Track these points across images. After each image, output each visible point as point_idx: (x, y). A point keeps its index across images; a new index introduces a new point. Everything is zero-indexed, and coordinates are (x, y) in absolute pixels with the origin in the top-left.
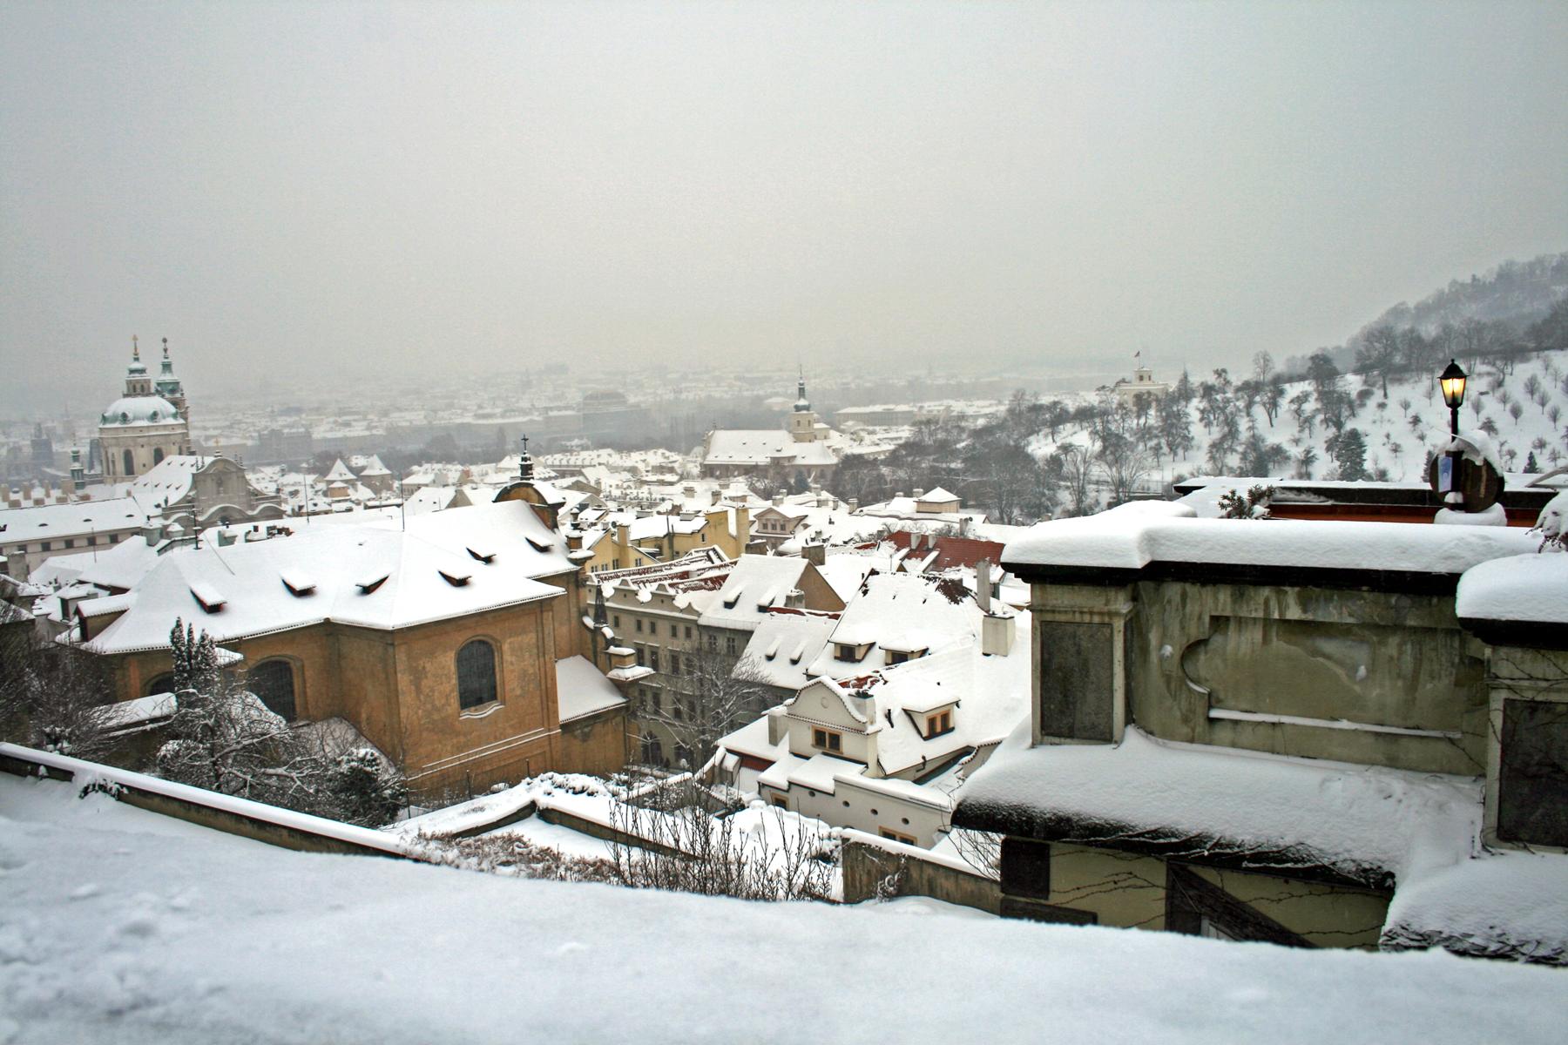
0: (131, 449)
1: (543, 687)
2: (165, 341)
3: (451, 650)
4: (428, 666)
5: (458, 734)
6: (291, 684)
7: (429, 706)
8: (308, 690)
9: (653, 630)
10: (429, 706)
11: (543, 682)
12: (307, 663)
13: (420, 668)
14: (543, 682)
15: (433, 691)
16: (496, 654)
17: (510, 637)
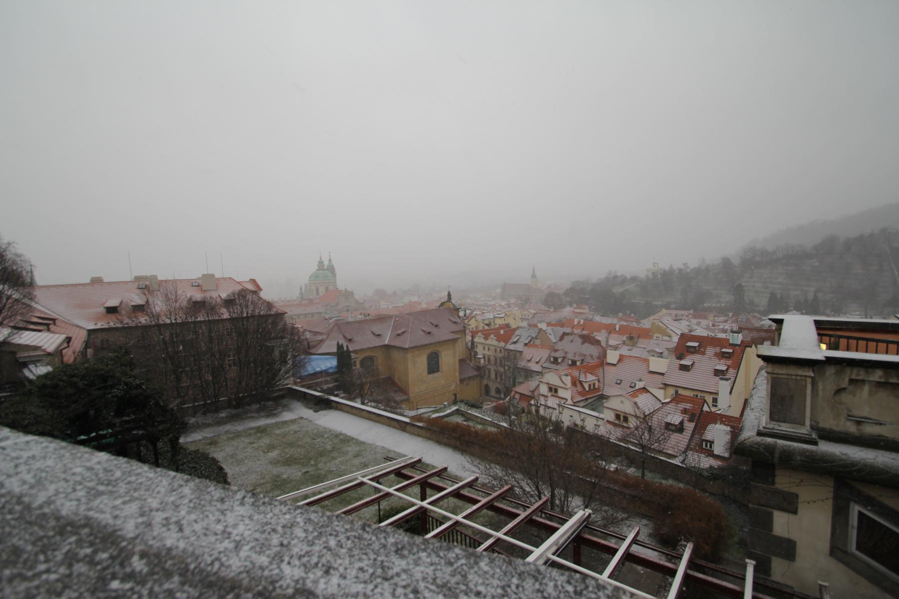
9: (489, 349)
16: (440, 357)
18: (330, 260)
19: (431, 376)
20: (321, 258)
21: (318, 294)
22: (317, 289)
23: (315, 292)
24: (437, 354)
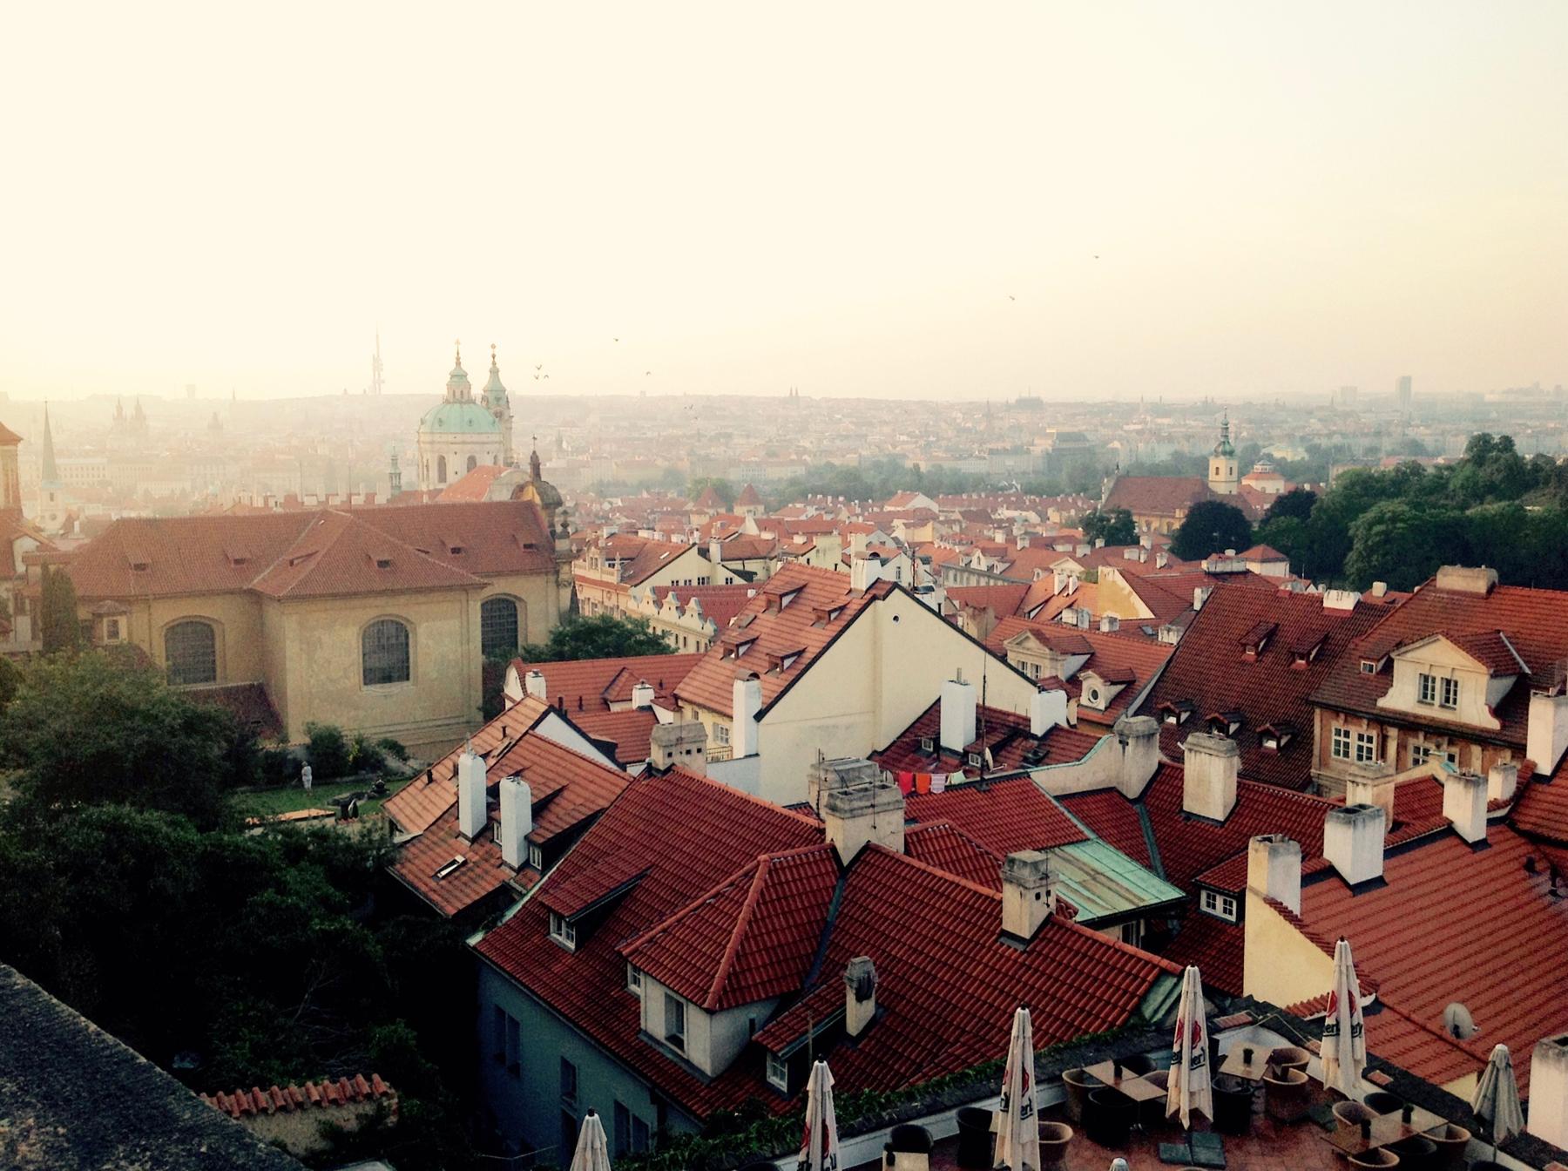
2: (493, 347)
7: (323, 677)
10: (323, 677)
16: (410, 635)
18: (494, 372)
19: (378, 690)
20: (458, 363)
21: (443, 478)
22: (442, 463)
23: (434, 474)
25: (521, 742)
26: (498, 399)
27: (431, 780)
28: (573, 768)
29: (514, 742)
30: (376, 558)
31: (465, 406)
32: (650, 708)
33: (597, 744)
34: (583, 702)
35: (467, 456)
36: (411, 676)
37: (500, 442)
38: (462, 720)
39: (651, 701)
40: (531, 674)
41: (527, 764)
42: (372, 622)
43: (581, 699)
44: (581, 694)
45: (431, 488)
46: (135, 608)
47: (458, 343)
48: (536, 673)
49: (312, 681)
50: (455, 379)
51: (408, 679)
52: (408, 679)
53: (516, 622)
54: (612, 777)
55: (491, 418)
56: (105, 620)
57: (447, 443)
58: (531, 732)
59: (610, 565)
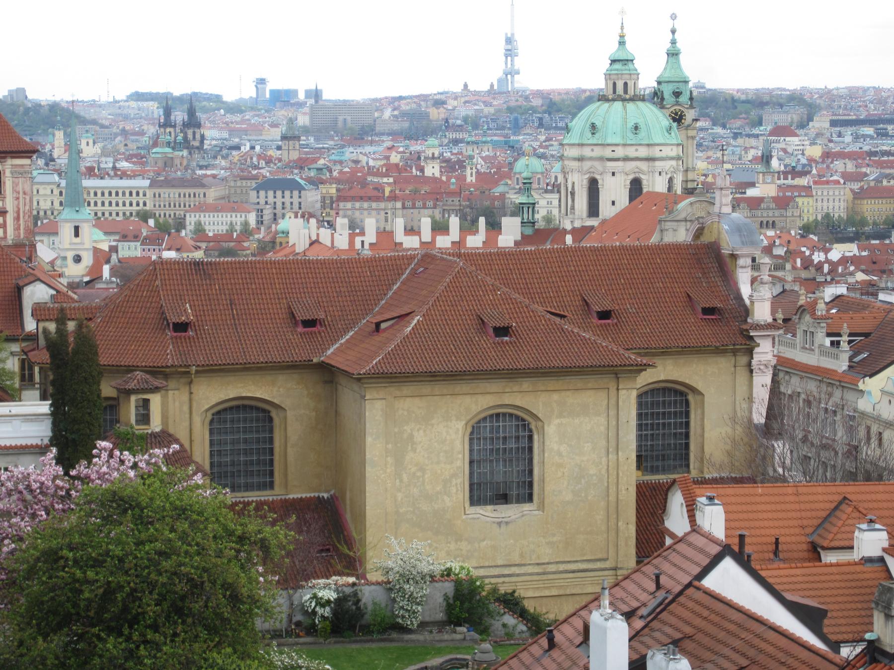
0: (598, 177)
1: (612, 498)
2: (674, 17)
3: (458, 419)
4: (419, 436)
5: (459, 539)
6: (271, 440)
7: (415, 491)
8: (289, 450)
10: (415, 491)
11: (613, 490)
12: (290, 414)
13: (405, 436)
14: (613, 490)
15: (422, 469)
16: (536, 437)
17: (560, 416)
18: (673, 54)
19: (488, 512)
20: (622, 43)
21: (593, 209)
22: (593, 187)
23: (582, 202)
24: (525, 426)
25: (682, 599)
26: (677, 94)
27: (552, 644)
28: (757, 641)
29: (670, 598)
30: (492, 323)
31: (630, 106)
32: (881, 560)
33: (795, 608)
34: (780, 547)
35: (631, 177)
36: (535, 497)
37: (678, 158)
38: (607, 565)
39: (884, 550)
40: (703, 500)
41: (688, 630)
42: (483, 415)
43: (777, 539)
44: (777, 532)
45: (578, 224)
46: (172, 384)
47: (623, 12)
48: (711, 499)
49: (400, 496)
50: (617, 66)
51: (530, 498)
52: (530, 498)
53: (687, 424)
54: (816, 661)
55: (666, 122)
56: (133, 398)
57: (601, 159)
58: (696, 583)
59: (832, 343)
